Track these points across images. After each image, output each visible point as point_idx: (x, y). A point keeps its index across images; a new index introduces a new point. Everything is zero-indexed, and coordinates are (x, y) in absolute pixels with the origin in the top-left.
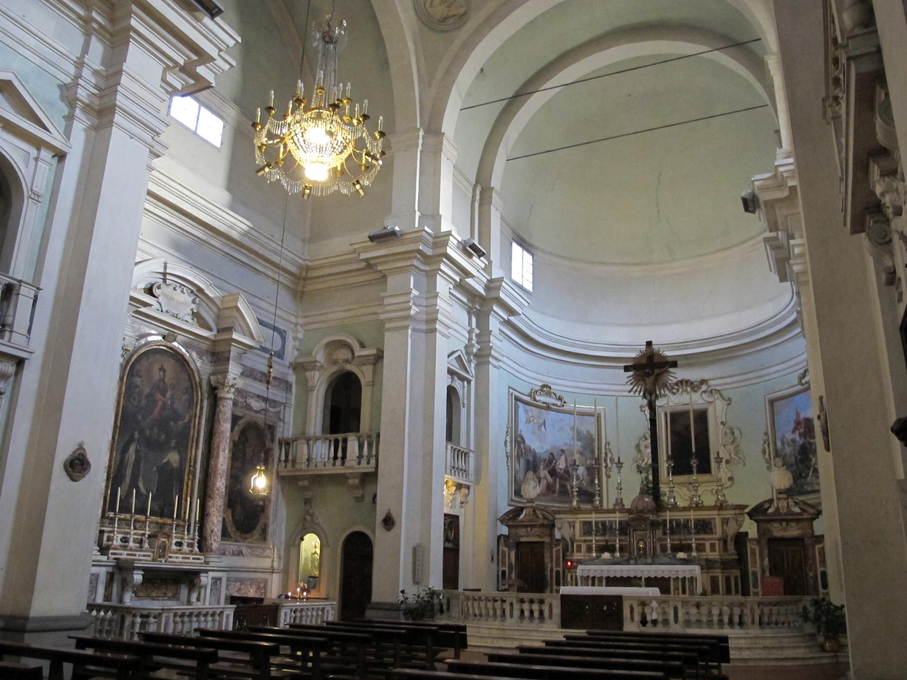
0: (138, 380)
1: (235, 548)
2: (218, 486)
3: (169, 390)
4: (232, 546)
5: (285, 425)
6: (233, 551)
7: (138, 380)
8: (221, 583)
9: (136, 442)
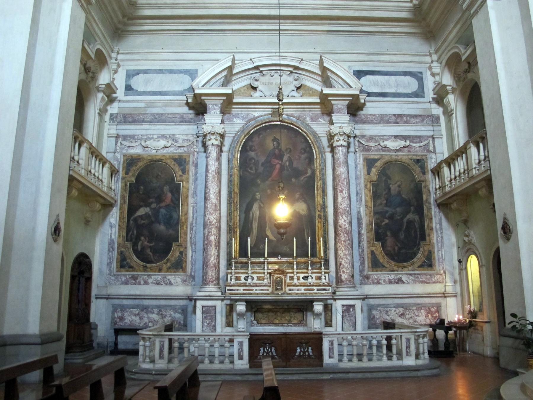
0: (252, 154)
1: (391, 277)
2: (340, 223)
3: (286, 154)
4: (387, 275)
5: (438, 155)
6: (389, 279)
7: (252, 154)
8: (354, 310)
9: (258, 201)
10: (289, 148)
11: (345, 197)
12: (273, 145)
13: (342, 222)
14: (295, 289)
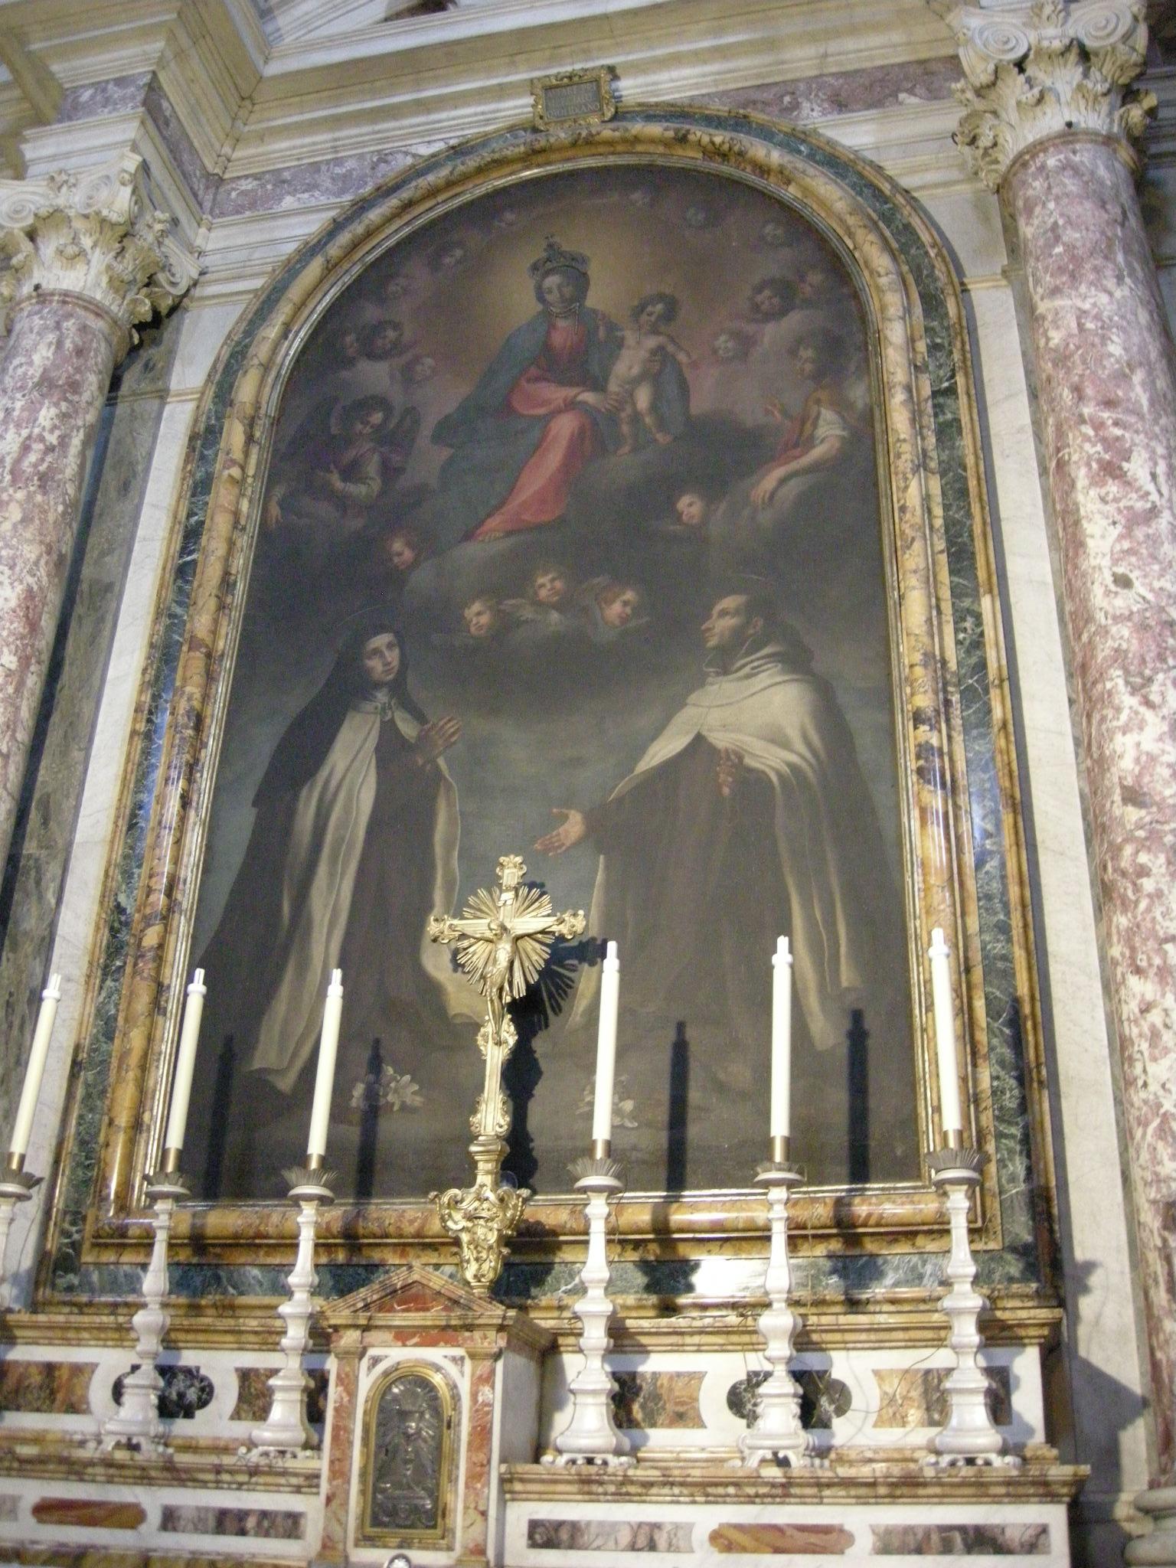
3: (630, 337)
9: (382, 697)
10: (661, 297)
11: (1153, 512)
12: (541, 297)
13: (1149, 744)
14: (608, 1530)
